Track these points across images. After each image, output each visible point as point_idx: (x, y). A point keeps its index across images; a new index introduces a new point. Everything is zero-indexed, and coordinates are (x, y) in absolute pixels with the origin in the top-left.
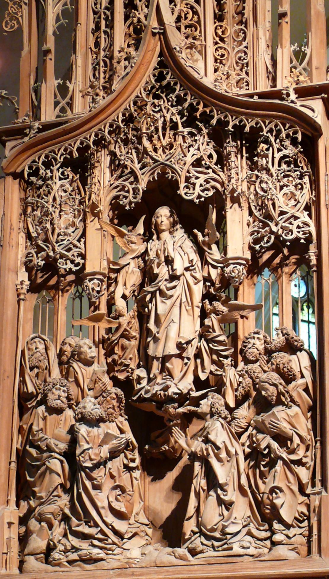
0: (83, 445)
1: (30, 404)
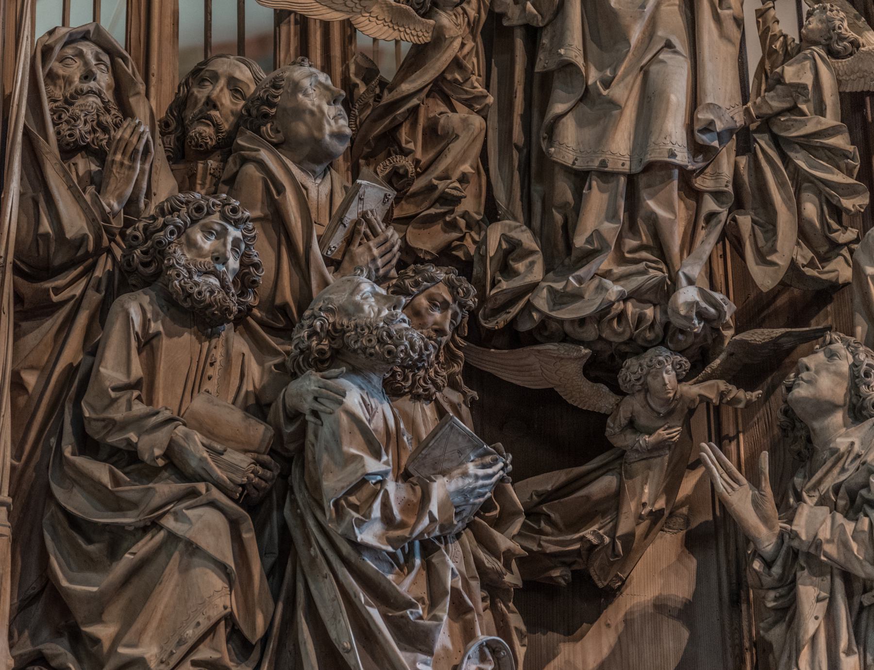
0: (355, 457)
1: (57, 290)
